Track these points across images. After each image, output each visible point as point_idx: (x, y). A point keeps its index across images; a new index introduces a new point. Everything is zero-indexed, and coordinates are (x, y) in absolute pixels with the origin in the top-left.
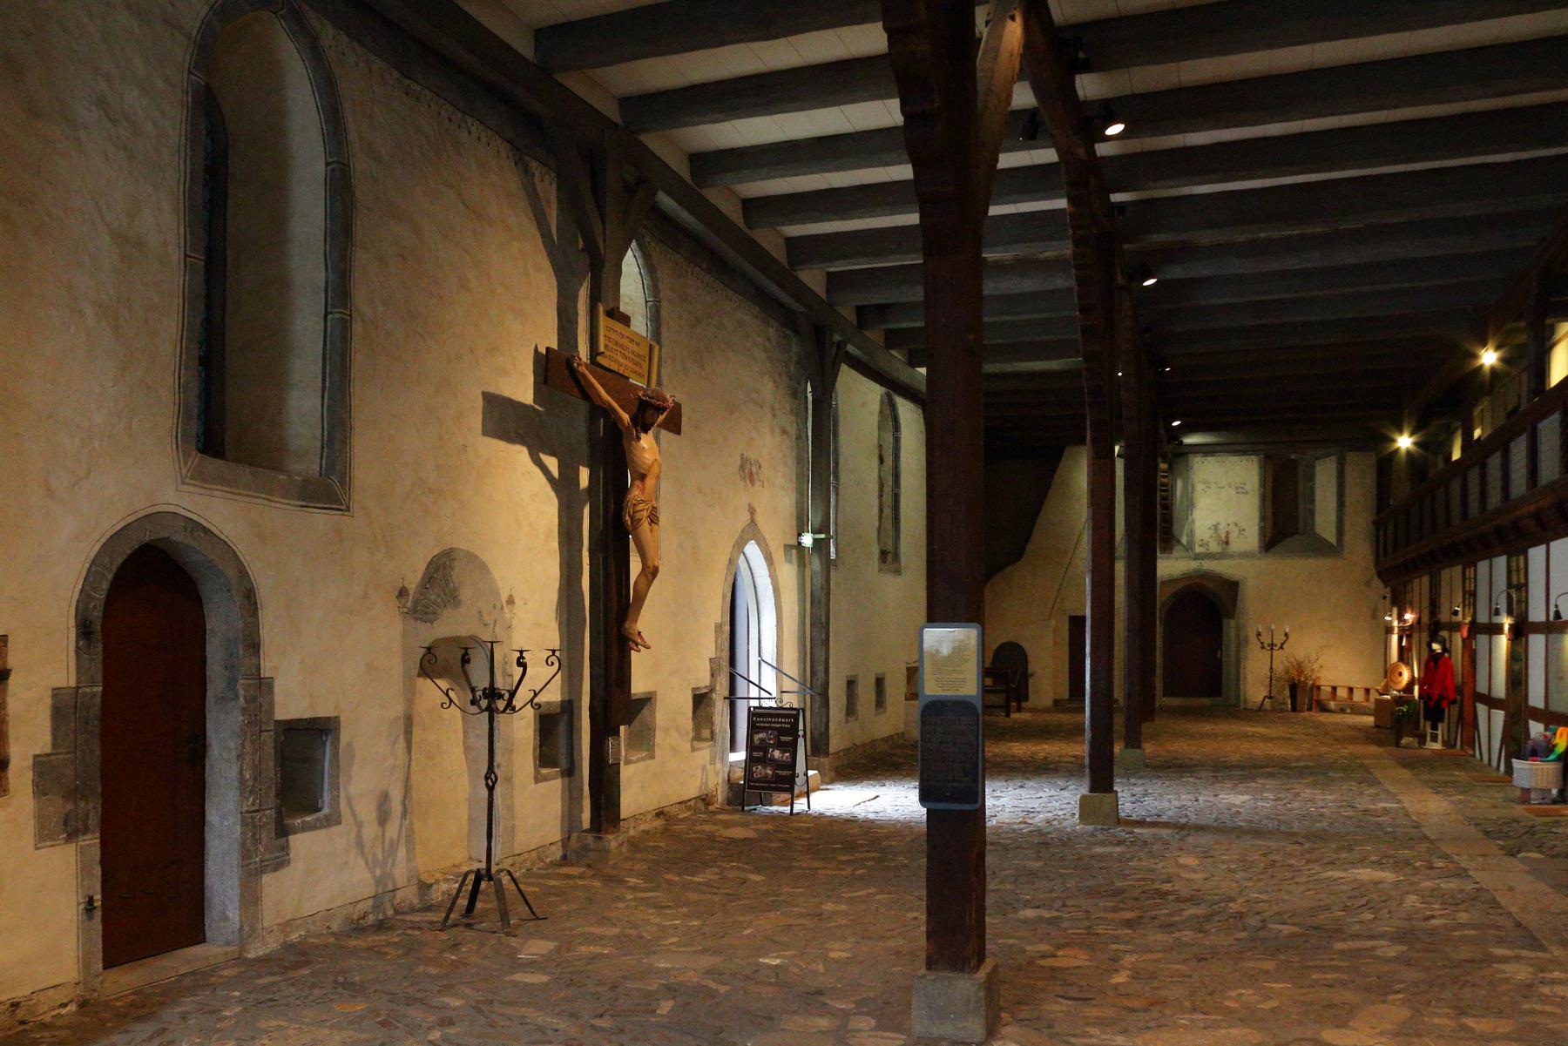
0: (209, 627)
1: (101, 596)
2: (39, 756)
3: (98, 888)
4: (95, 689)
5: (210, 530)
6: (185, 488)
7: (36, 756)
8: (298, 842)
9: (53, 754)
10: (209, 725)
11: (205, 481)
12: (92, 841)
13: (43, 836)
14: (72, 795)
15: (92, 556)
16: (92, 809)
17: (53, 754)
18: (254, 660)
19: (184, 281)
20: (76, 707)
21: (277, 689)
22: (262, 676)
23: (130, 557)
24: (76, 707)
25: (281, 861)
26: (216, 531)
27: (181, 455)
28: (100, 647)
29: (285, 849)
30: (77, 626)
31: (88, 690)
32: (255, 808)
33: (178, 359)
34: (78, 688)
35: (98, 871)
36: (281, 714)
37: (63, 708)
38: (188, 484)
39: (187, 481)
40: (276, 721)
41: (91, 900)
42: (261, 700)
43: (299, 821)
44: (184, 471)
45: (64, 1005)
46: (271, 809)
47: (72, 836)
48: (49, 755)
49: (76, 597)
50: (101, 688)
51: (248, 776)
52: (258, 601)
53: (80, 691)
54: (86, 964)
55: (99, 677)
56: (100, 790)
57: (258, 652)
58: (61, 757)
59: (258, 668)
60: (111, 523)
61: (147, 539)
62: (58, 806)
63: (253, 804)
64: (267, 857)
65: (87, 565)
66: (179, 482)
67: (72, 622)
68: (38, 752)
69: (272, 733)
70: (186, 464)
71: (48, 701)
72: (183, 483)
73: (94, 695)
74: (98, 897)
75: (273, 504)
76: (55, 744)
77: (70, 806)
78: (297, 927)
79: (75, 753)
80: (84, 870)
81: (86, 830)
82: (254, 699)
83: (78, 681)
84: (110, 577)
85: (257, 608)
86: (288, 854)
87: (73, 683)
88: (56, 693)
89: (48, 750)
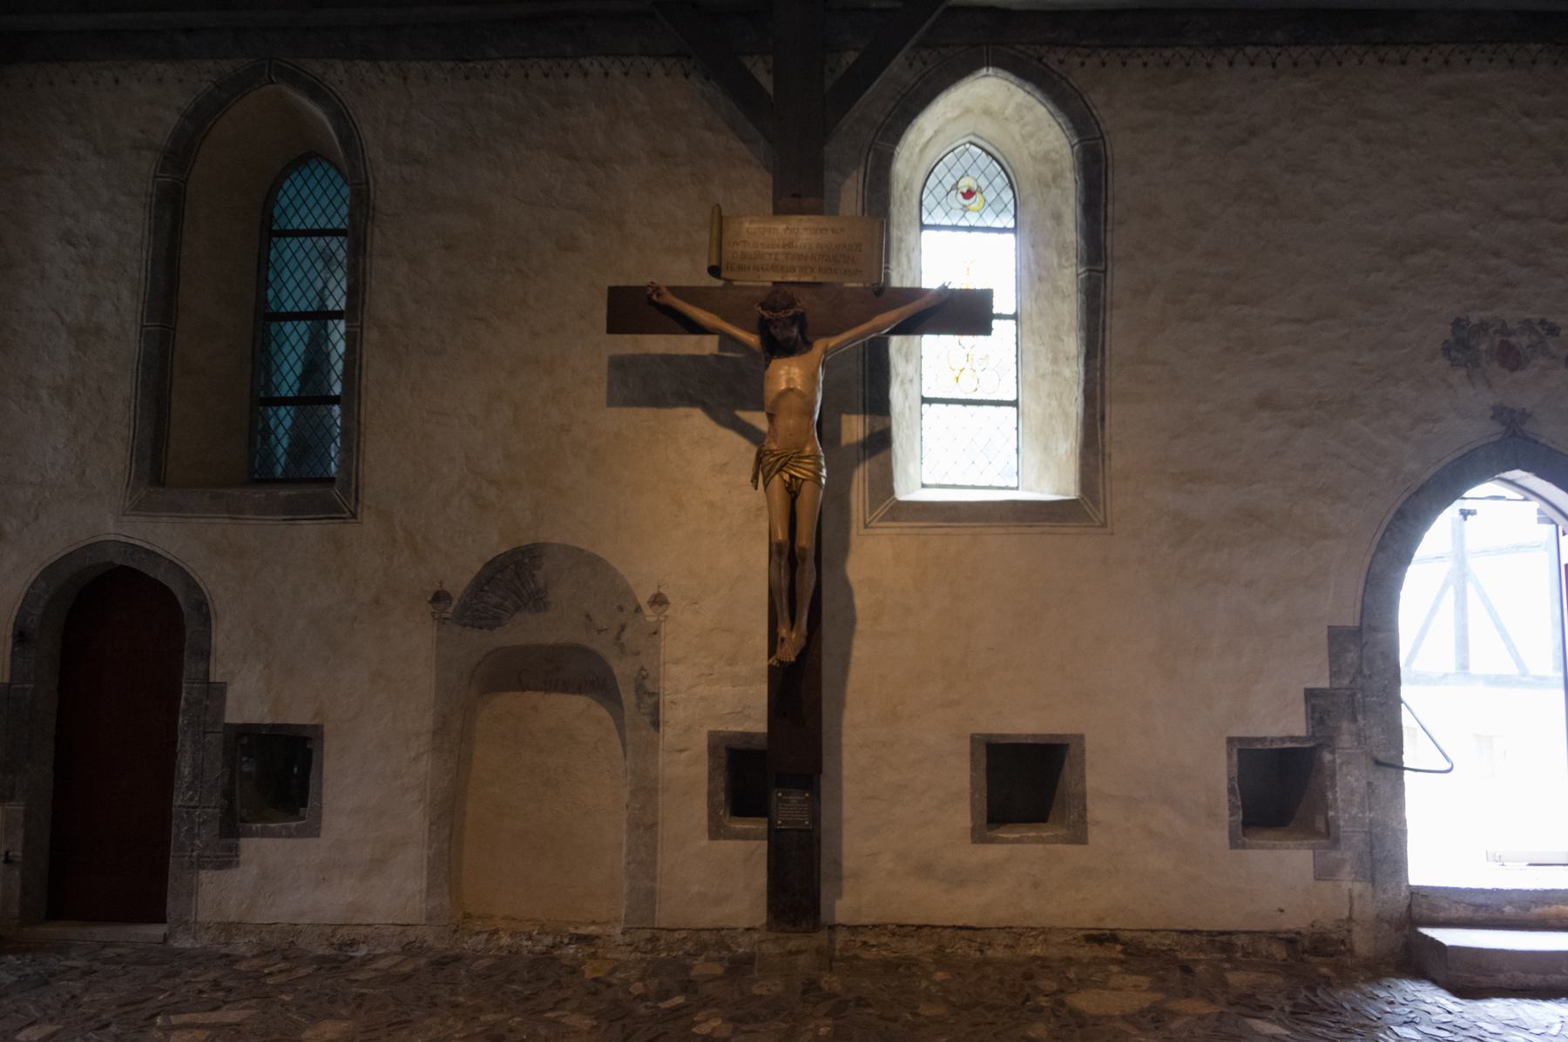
5: (153, 552)
6: (125, 519)
8: (249, 847)
19: (140, 348)
22: (212, 680)
25: (227, 860)
26: (160, 552)
29: (234, 850)
32: (192, 804)
33: (132, 413)
36: (233, 716)
38: (128, 515)
39: (127, 513)
42: (208, 703)
43: (259, 825)
44: (127, 505)
46: (215, 807)
49: (15, 613)
51: (186, 773)
52: (212, 611)
63: (191, 799)
64: (208, 853)
65: (26, 589)
69: (221, 735)
70: (130, 498)
72: (124, 515)
75: (241, 522)
78: (246, 933)
85: (210, 619)
86: (237, 856)
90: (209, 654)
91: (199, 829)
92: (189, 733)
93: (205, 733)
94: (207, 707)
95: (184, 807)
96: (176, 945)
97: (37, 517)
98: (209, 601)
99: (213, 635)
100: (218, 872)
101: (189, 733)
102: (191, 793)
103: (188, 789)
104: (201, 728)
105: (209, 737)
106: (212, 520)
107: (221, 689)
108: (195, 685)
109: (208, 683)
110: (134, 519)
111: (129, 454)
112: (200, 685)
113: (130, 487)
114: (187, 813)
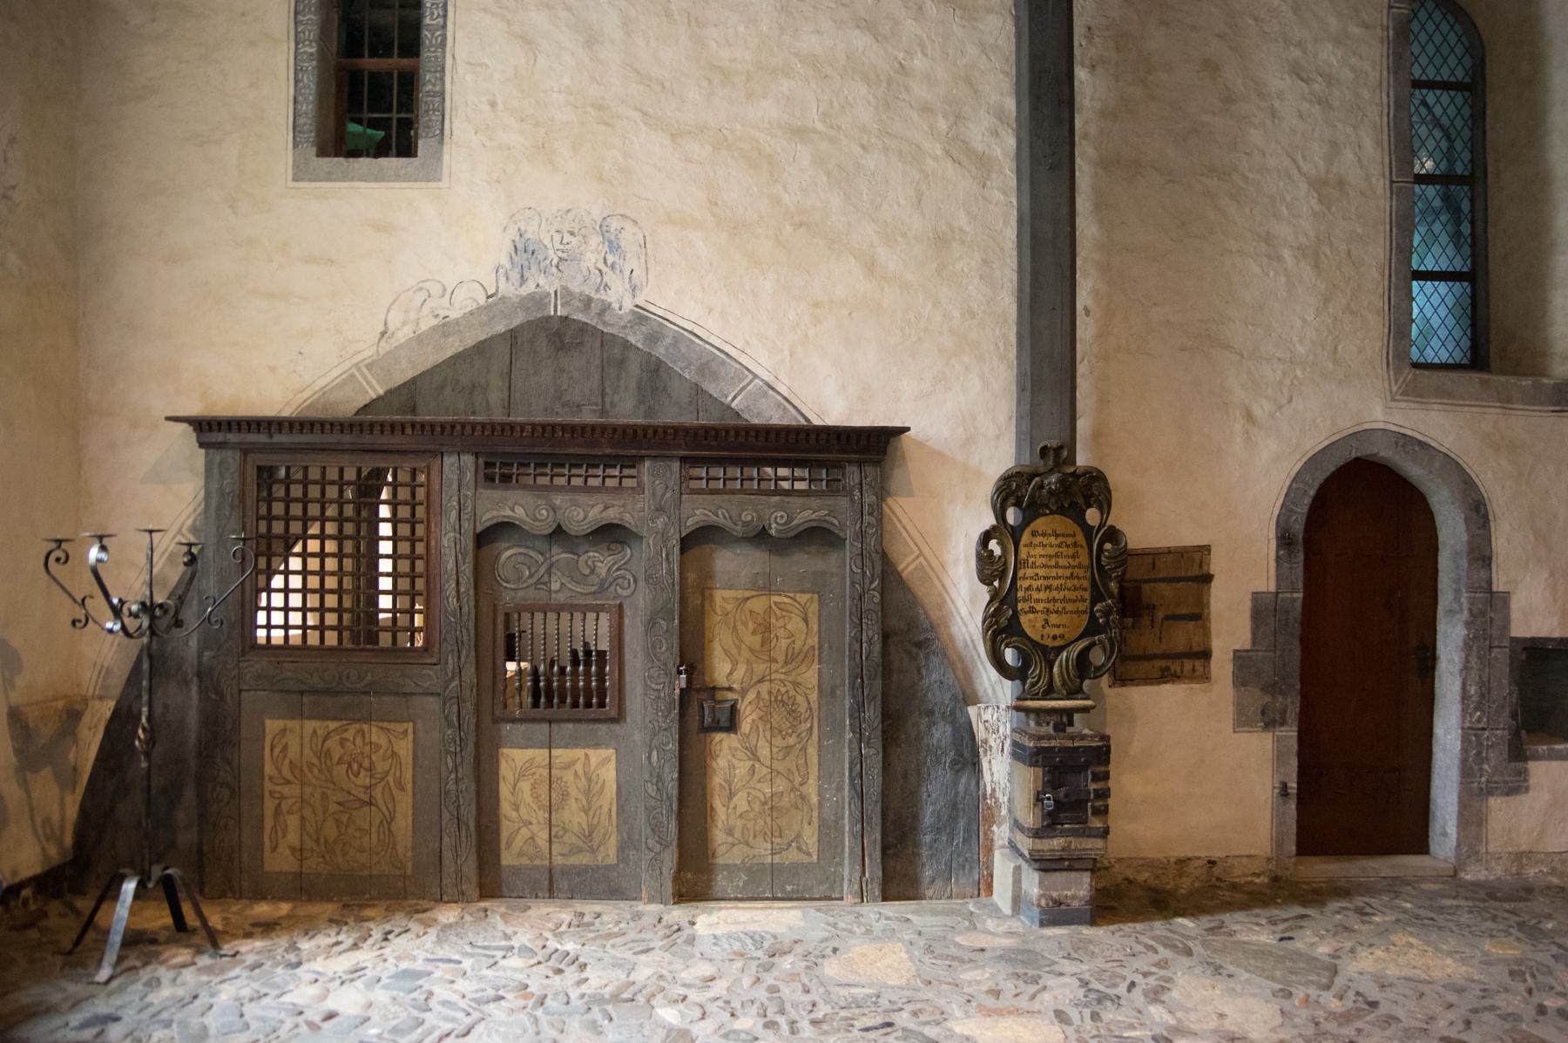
0: (1441, 539)
1: (1303, 509)
2: (1238, 651)
3: (1294, 776)
4: (1295, 595)
5: (1426, 444)
6: (1394, 404)
7: (1236, 651)
9: (1253, 651)
10: (1439, 637)
11: (1421, 396)
12: (1290, 733)
13: (1242, 721)
14: (1271, 688)
15: (1293, 473)
16: (1293, 705)
17: (1253, 651)
18: (1483, 574)
20: (1275, 610)
21: (1515, 605)
22: (1494, 589)
23: (1333, 474)
24: (1275, 610)
26: (1433, 444)
27: (1391, 373)
28: (1301, 557)
30: (1277, 537)
31: (1288, 595)
33: (1386, 283)
34: (1277, 593)
35: (1294, 762)
37: (1263, 610)
38: (1398, 401)
39: (1398, 397)
40: (1513, 639)
41: (1284, 787)
42: (1492, 615)
44: (1395, 389)
45: (1258, 875)
47: (1269, 725)
48: (1247, 651)
49: (1276, 512)
50: (1301, 595)
51: (1473, 692)
52: (1491, 513)
53: (1280, 596)
54: (1279, 843)
55: (1300, 585)
56: (1298, 687)
57: (1490, 564)
58: (1260, 654)
59: (1490, 583)
60: (1314, 442)
61: (1353, 455)
62: (1256, 698)
65: (1288, 483)
66: (1389, 398)
67: (1272, 535)
68: (1237, 647)
70: (1396, 383)
71: (1248, 604)
72: (1393, 400)
73: (1294, 600)
74: (1293, 785)
75: (1511, 412)
76: (1254, 642)
77: (1268, 699)
79: (1275, 652)
80: (1280, 758)
81: (1283, 723)
82: (1483, 613)
83: (1278, 586)
84: (1312, 493)
87: (1272, 588)
88: (1256, 597)
89: (1248, 646)
90: (1490, 559)
91: (1487, 753)
92: (1474, 648)
93: (1491, 647)
94: (1491, 620)
95: (1472, 729)
96: (1468, 877)
97: (1290, 400)
98: (1487, 502)
99: (1493, 539)
100: (1507, 798)
101: (1474, 648)
102: (1478, 713)
103: (1476, 709)
104: (1487, 643)
105: (1495, 651)
106: (1486, 410)
107: (1505, 598)
108: (1478, 595)
109: (1491, 592)
110: (1404, 405)
111: (1386, 331)
112: (1482, 595)
113: (1391, 367)
114: (1475, 735)
